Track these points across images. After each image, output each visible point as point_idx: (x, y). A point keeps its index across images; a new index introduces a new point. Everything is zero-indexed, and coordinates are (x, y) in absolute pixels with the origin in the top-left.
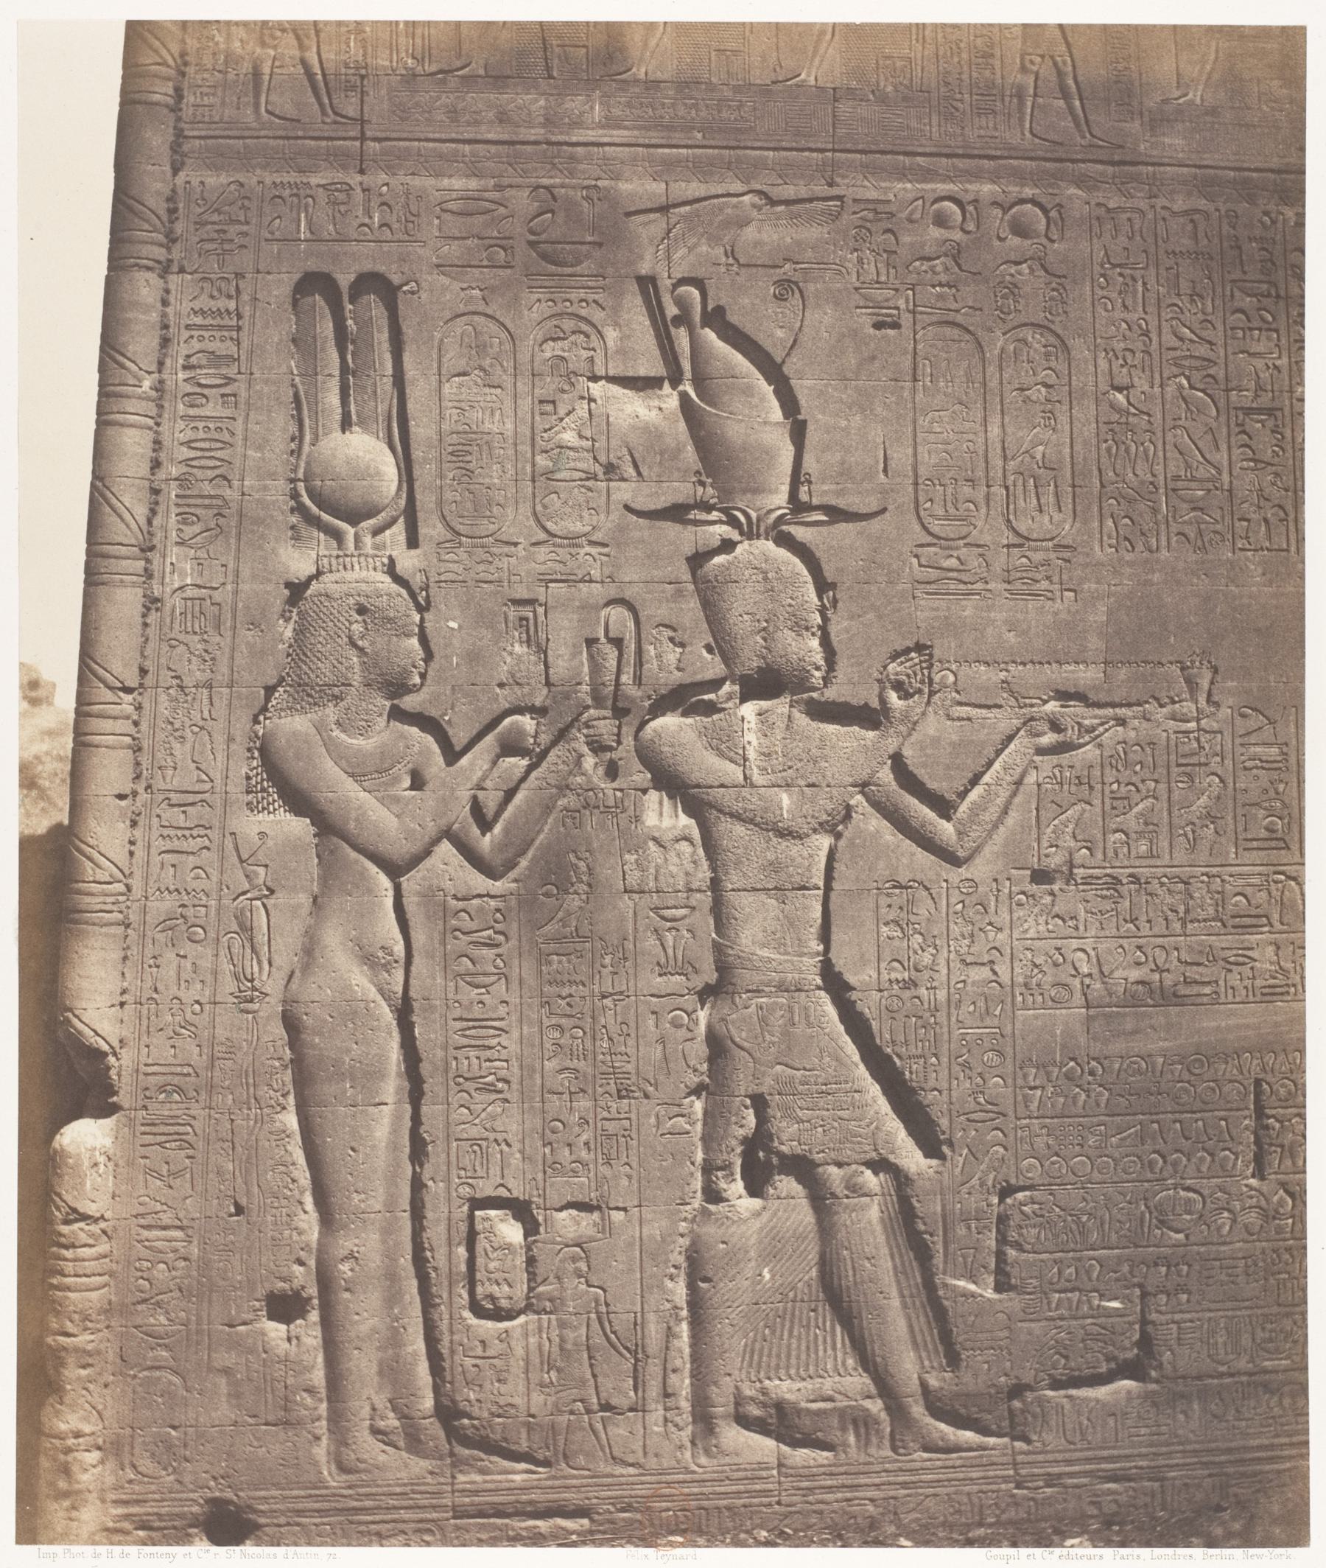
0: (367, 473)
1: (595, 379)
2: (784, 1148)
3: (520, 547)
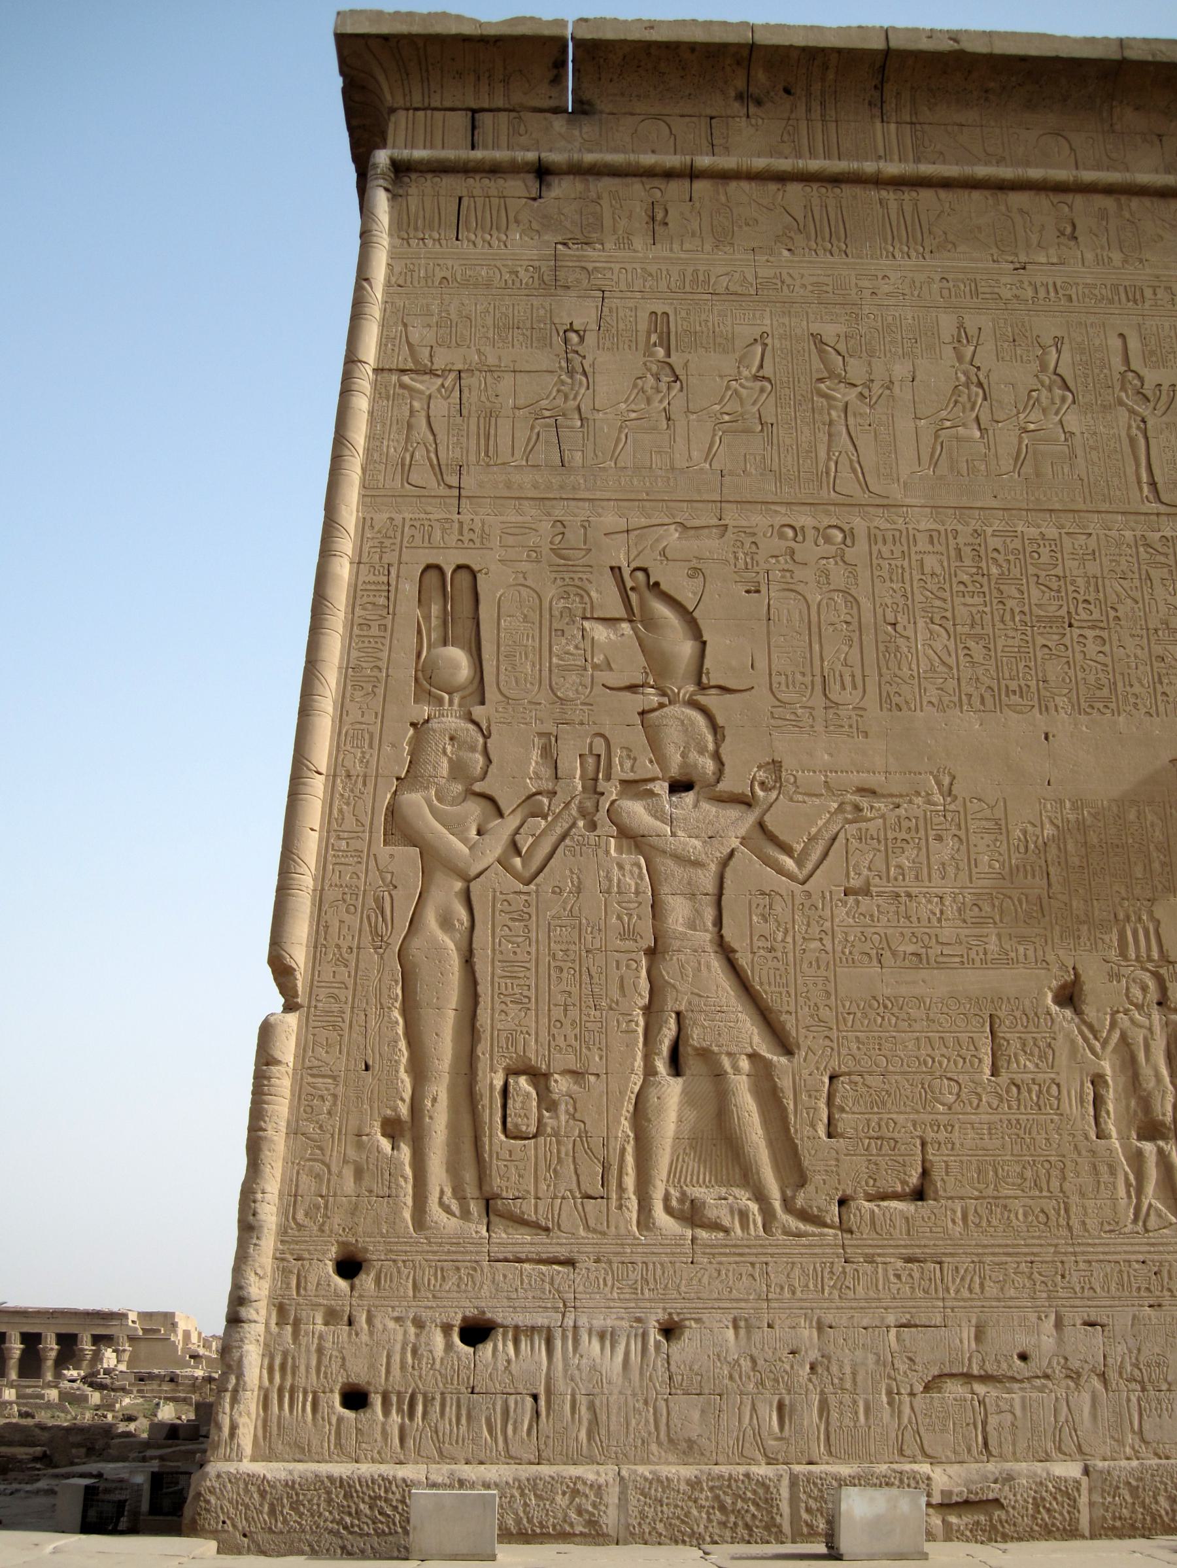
0: (457, 667)
1: (585, 618)
2: (695, 1043)
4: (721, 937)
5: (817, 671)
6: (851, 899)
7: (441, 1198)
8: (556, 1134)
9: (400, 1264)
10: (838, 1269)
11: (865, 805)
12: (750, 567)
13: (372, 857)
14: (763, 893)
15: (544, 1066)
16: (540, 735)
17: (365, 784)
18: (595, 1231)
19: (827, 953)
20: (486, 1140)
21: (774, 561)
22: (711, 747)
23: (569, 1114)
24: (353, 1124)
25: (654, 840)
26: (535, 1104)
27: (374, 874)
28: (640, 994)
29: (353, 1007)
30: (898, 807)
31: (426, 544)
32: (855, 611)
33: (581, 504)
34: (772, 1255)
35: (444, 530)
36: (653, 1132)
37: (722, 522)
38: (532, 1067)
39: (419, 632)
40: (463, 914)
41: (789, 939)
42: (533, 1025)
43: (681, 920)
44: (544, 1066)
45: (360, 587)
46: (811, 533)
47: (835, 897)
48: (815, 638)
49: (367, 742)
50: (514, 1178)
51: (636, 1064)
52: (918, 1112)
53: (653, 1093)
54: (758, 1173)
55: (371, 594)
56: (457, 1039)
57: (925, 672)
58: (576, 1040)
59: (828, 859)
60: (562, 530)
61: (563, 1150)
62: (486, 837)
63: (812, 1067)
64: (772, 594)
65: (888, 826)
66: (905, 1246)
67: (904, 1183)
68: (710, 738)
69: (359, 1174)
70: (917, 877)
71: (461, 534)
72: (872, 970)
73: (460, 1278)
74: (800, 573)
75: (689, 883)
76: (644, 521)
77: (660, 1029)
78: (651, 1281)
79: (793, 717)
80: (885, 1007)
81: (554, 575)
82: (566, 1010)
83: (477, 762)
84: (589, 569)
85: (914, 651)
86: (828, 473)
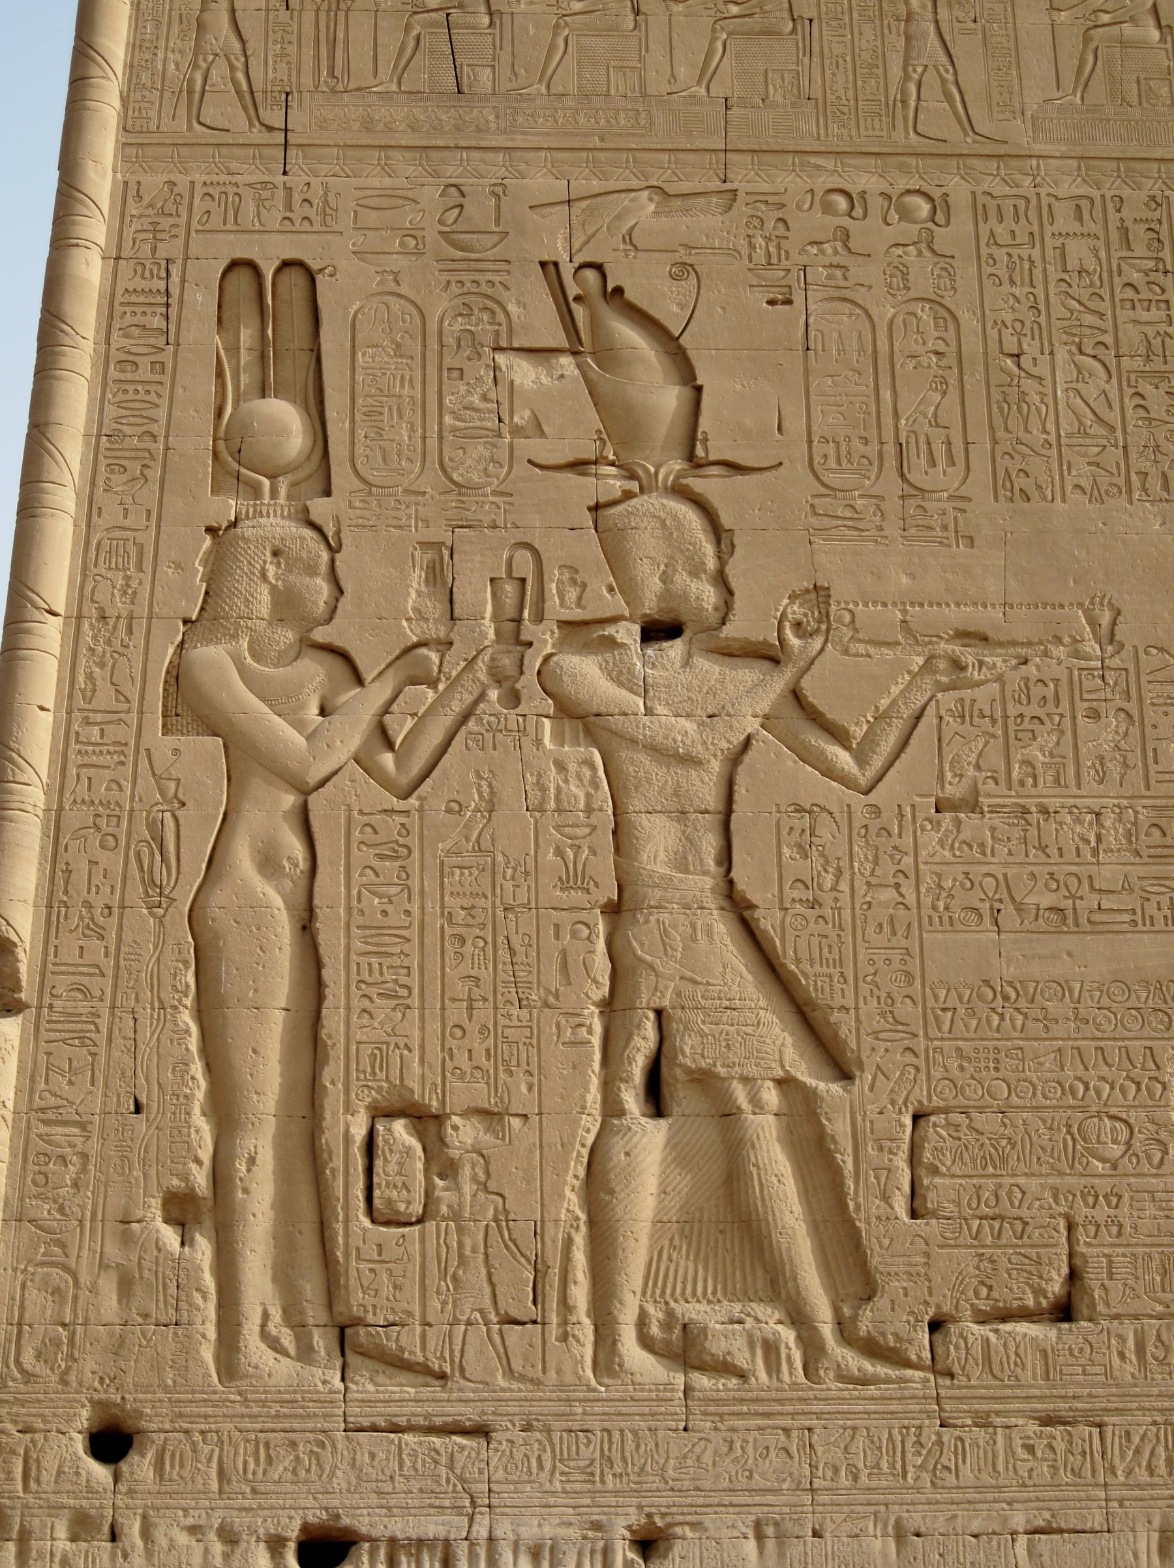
0: (283, 432)
1: (497, 349)
2: (688, 1062)
3: (427, 496)
4: (731, 883)
5: (888, 435)
6: (947, 817)
7: (263, 1326)
8: (456, 1215)
9: (197, 1437)
10: (929, 1437)
11: (970, 660)
12: (774, 260)
13: (143, 753)
14: (800, 809)
15: (435, 1103)
16: (425, 545)
17: (130, 631)
18: (522, 1378)
19: (907, 908)
20: (339, 1227)
21: (814, 250)
22: (711, 564)
23: (478, 1183)
24: (115, 1203)
25: (617, 722)
26: (420, 1165)
27: (146, 782)
28: (595, 981)
29: (113, 1007)
30: (1025, 663)
31: (230, 226)
32: (951, 335)
33: (490, 156)
34: (819, 1415)
35: (260, 202)
36: (619, 1211)
37: (728, 186)
38: (414, 1104)
39: (220, 374)
40: (296, 847)
41: (844, 886)
42: (417, 1033)
43: (662, 856)
44: (435, 1103)
45: (119, 299)
46: (876, 204)
47: (920, 815)
48: (885, 380)
49: (133, 560)
50: (386, 1290)
51: (589, 1098)
52: (1061, 1174)
53: (617, 1147)
54: (795, 1279)
55: (139, 310)
56: (288, 1059)
57: (1070, 435)
58: (488, 1059)
59: (908, 750)
60: (460, 200)
61: (468, 1242)
62: (335, 718)
63: (885, 1100)
64: (811, 307)
65: (1008, 694)
66: (1041, 1398)
67: (1039, 1292)
68: (709, 549)
69: (126, 1286)
70: (1057, 781)
71: (289, 207)
72: (982, 936)
73: (297, 1458)
74: (858, 271)
75: (676, 794)
76: (596, 185)
77: (629, 1038)
78: (617, 1460)
79: (848, 513)
80: (1006, 998)
81: (445, 277)
82: (470, 1008)
83: (319, 593)
84: (504, 266)
85: (1049, 400)
86: (904, 102)
